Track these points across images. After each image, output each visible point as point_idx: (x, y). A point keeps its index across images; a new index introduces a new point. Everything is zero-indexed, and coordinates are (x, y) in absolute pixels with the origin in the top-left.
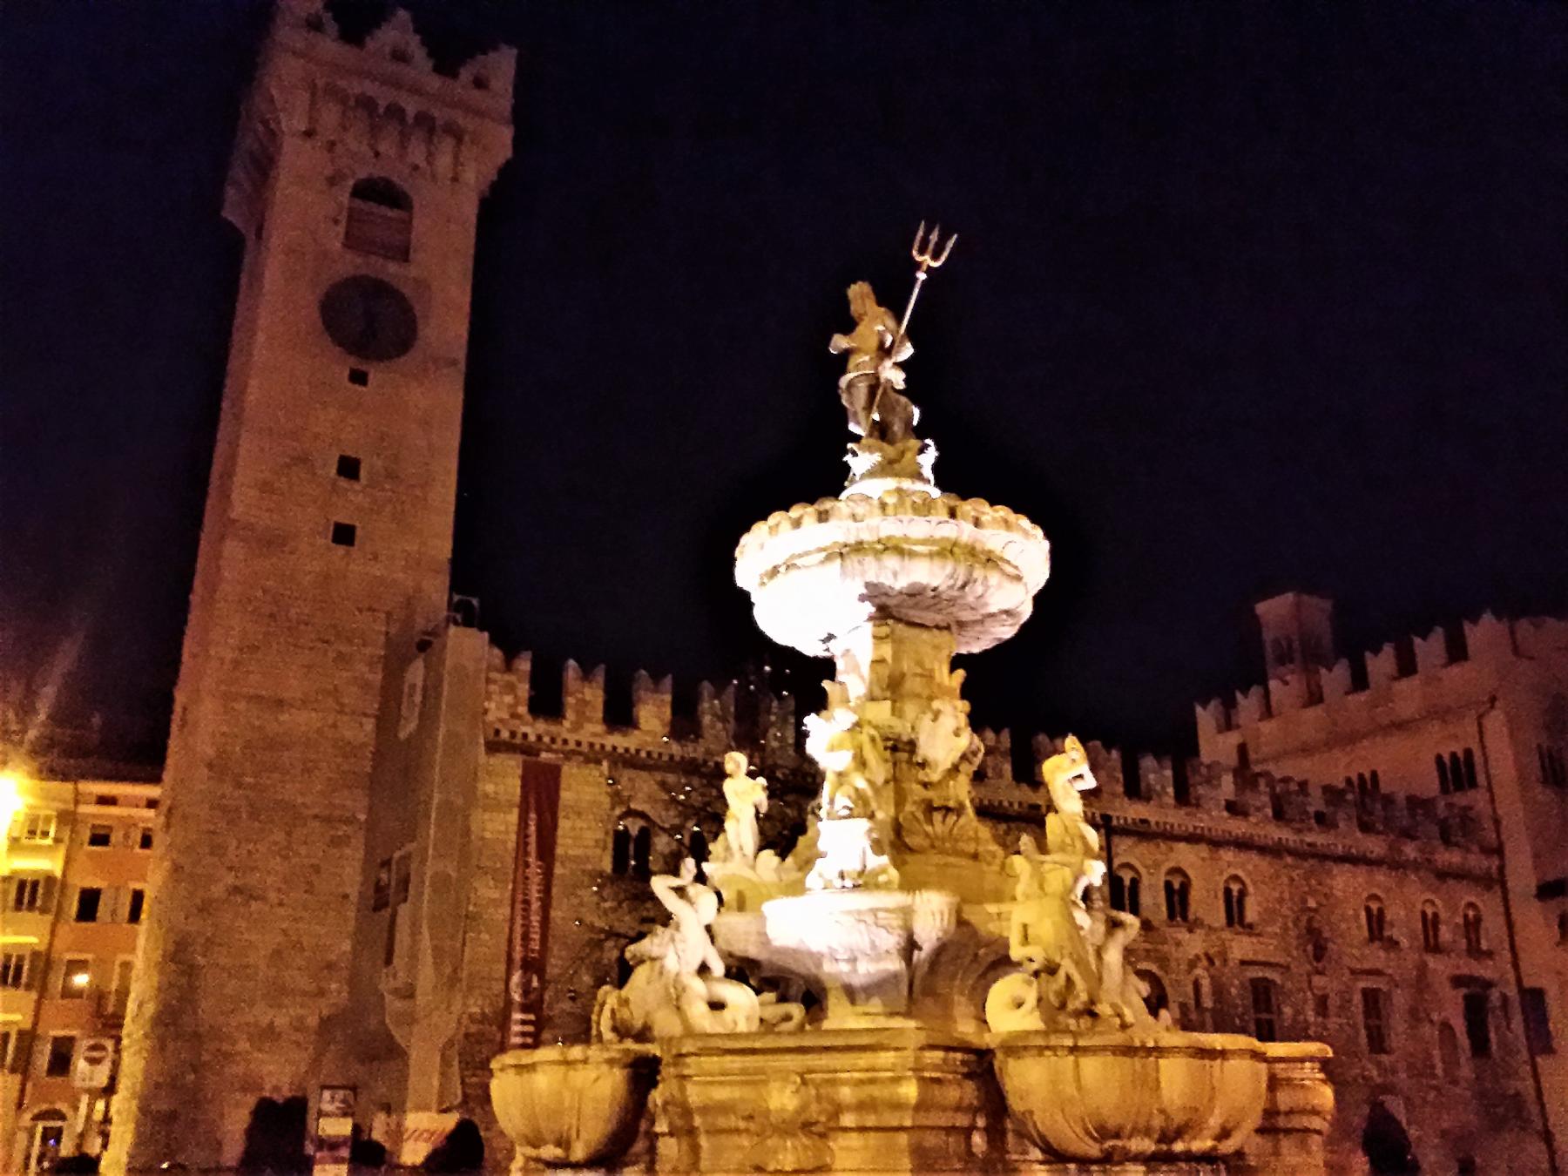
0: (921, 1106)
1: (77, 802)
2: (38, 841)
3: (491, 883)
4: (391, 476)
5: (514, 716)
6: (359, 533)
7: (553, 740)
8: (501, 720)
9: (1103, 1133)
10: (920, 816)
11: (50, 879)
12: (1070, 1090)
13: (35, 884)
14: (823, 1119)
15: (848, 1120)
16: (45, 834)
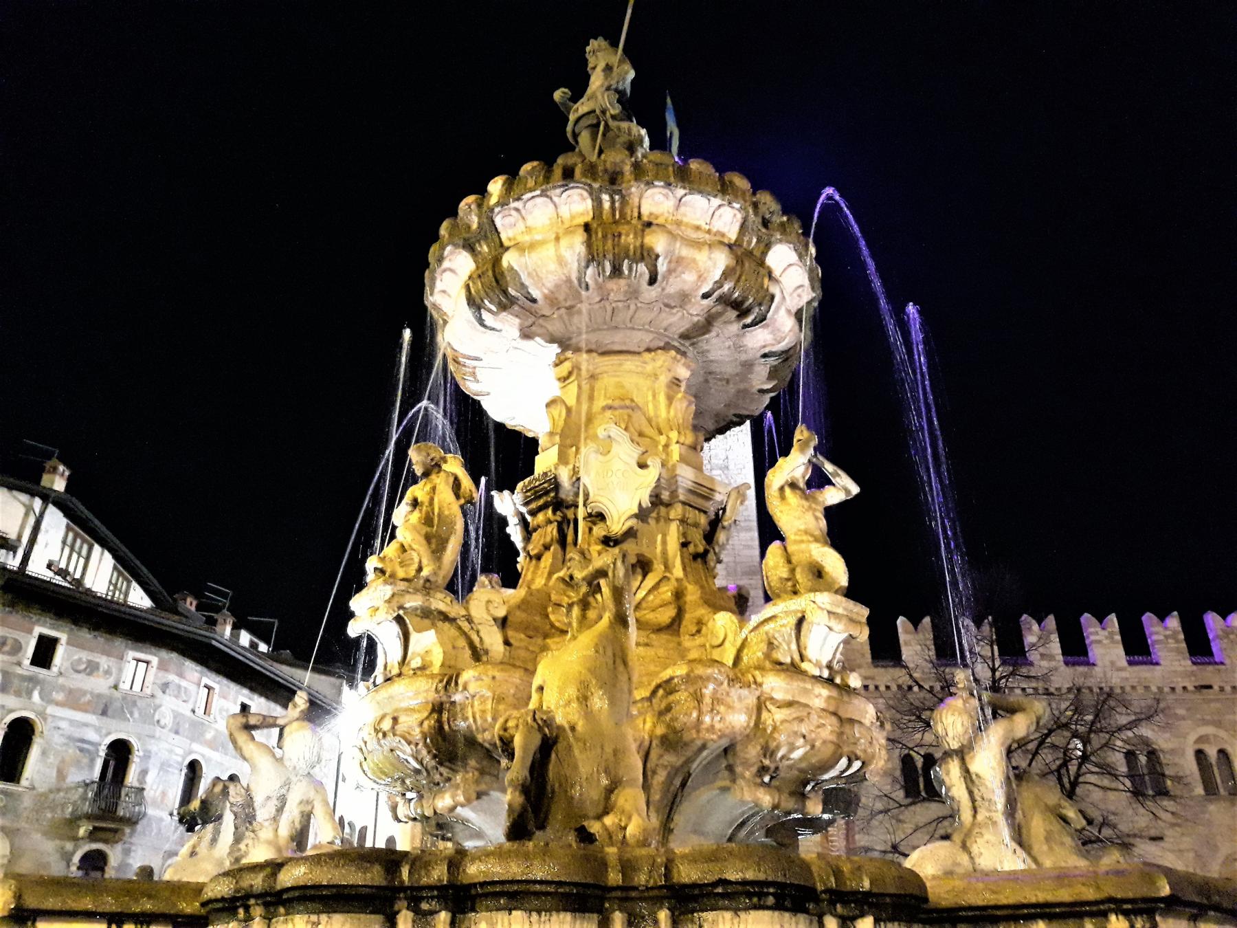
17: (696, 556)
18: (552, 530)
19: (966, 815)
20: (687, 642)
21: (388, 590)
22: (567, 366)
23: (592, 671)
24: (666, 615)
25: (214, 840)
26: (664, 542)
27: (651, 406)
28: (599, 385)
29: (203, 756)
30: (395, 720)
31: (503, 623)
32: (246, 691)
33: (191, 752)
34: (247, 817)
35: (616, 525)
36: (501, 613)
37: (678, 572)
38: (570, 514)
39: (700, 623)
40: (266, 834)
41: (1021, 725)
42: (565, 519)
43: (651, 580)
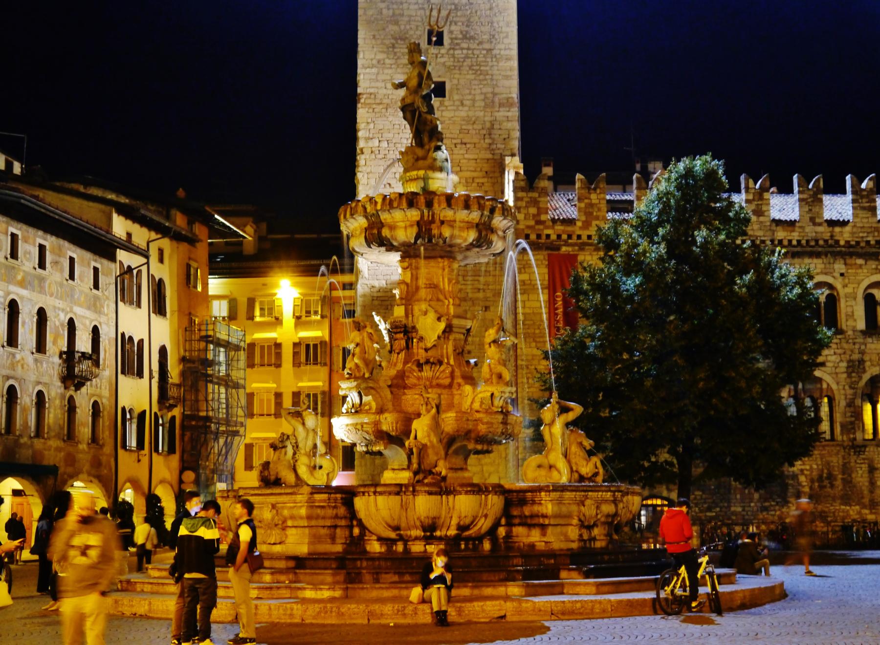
0: (309, 518)
1: (331, 290)
2: (313, 317)
3: (534, 344)
4: (465, 37)
5: (539, 222)
6: (448, 87)
7: (570, 237)
8: (528, 227)
9: (396, 528)
10: (415, 368)
11: (323, 343)
12: (373, 509)
13: (315, 346)
14: (280, 522)
15: (289, 523)
16: (316, 313)
17: (459, 354)
18: (403, 343)
19: (549, 445)
20: (455, 392)
21: (355, 384)
22: (406, 264)
23: (431, 429)
24: (447, 381)
25: (285, 454)
26: (447, 349)
27: (441, 284)
28: (419, 272)
29: (17, 294)
30: (362, 426)
31: (389, 386)
32: (40, 233)
33: (9, 293)
34: (296, 446)
35: (429, 345)
36: (389, 383)
37: (452, 362)
38: (410, 335)
39: (459, 385)
40: (303, 452)
41: (571, 416)
42: (408, 338)
43: (442, 368)
